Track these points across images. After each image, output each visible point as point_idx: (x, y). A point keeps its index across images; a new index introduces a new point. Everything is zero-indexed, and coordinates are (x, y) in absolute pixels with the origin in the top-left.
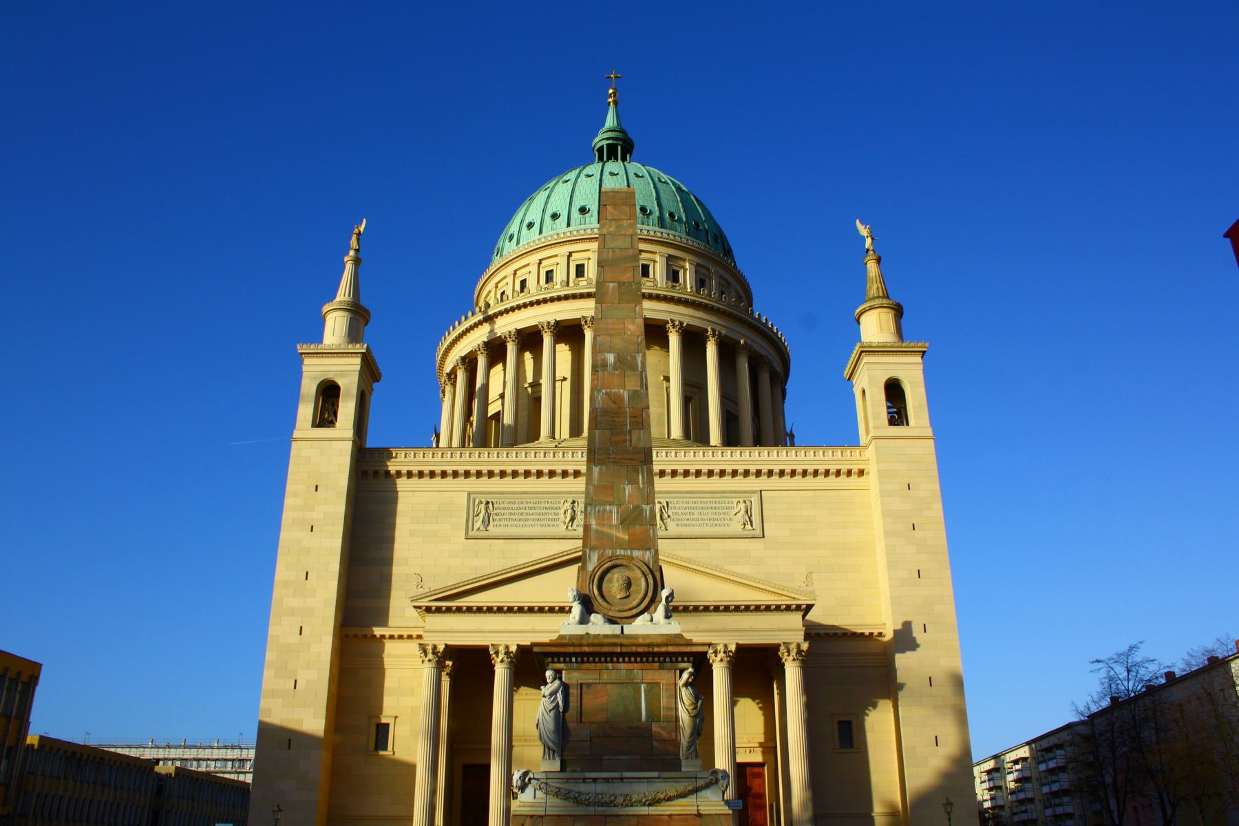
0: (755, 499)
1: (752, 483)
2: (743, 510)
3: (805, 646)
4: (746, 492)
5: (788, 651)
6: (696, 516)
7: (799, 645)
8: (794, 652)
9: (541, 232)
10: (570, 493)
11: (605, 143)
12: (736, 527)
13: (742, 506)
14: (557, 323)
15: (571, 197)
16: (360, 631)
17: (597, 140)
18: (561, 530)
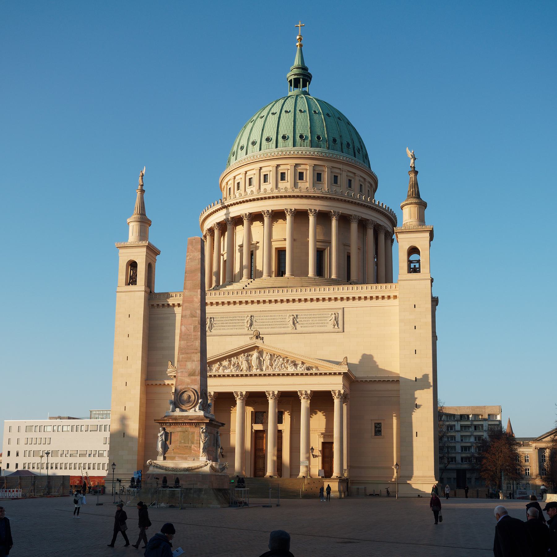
0: (340, 312)
1: (339, 304)
2: (334, 318)
3: (342, 392)
4: (336, 309)
5: (335, 394)
6: (311, 322)
7: (339, 391)
8: (337, 394)
9: (246, 154)
10: (250, 312)
11: (292, 77)
12: (330, 327)
13: (333, 316)
14: (250, 214)
15: (263, 130)
16: (154, 383)
17: (288, 75)
18: (245, 331)
